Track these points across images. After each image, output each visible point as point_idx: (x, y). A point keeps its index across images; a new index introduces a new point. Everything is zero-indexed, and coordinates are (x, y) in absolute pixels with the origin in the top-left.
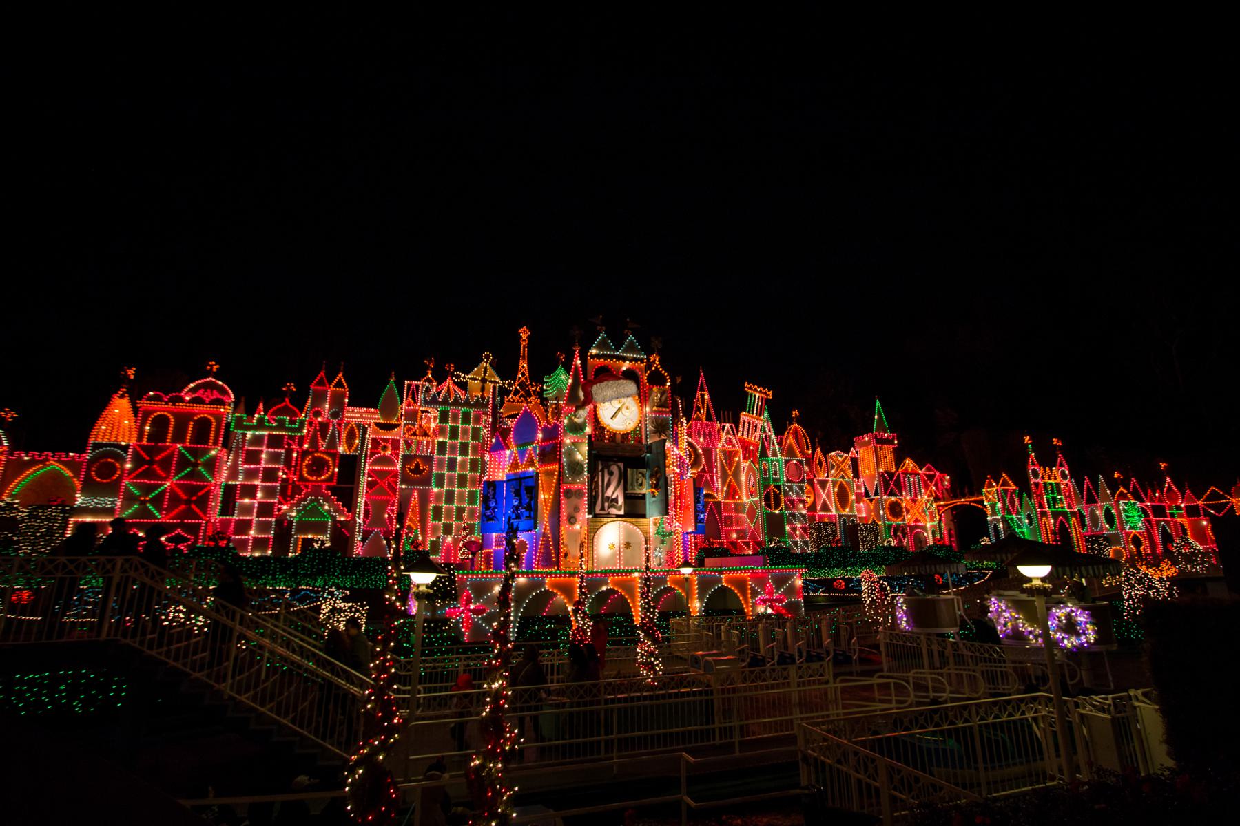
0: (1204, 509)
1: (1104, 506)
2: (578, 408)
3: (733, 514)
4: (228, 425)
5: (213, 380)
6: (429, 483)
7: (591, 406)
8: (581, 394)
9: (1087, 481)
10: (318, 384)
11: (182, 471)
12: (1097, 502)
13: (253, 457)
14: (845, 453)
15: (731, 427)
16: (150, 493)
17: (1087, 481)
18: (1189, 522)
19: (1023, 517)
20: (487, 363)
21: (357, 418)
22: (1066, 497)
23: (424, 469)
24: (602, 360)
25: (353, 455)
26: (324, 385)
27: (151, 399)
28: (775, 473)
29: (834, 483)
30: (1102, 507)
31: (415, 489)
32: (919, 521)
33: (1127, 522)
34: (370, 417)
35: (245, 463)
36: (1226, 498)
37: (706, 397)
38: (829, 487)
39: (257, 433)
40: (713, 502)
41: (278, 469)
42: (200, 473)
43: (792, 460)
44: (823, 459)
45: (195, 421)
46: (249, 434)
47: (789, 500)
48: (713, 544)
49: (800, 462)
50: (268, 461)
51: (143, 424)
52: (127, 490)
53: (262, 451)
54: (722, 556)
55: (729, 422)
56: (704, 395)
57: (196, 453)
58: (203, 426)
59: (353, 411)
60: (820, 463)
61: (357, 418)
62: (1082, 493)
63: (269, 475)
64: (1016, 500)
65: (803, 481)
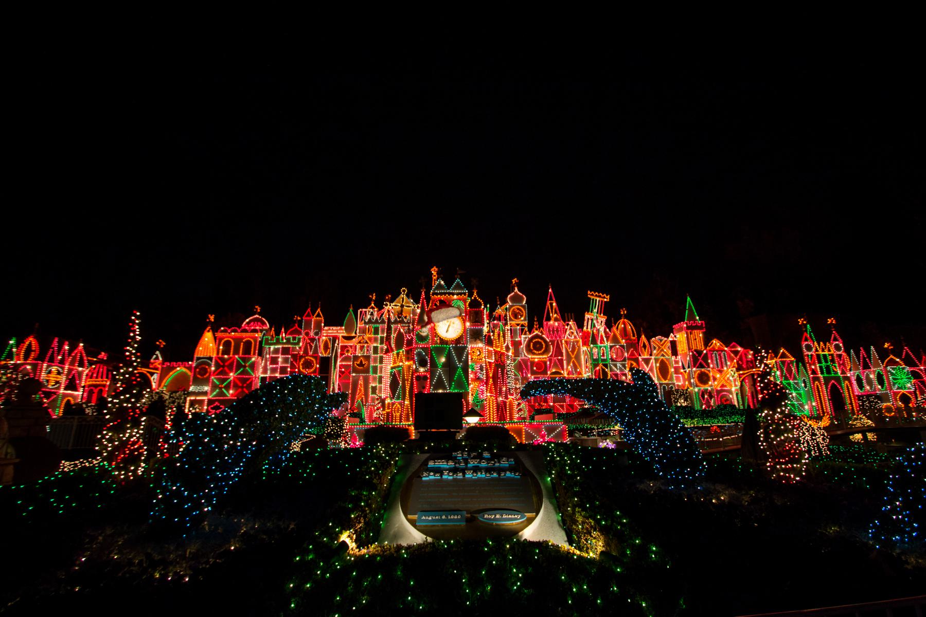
1: (876, 370)
2: (422, 327)
4: (261, 342)
5: (258, 316)
6: (368, 372)
7: (432, 325)
8: (426, 318)
9: (862, 352)
10: (307, 316)
12: (870, 368)
13: (274, 361)
14: (665, 337)
16: (223, 383)
17: (862, 352)
19: (799, 381)
20: (404, 294)
21: (335, 333)
22: (839, 365)
23: (365, 364)
24: (439, 296)
25: (327, 357)
26: (310, 316)
27: (222, 331)
28: (603, 355)
29: (656, 360)
30: (874, 372)
31: (360, 376)
32: (726, 386)
33: (894, 384)
34: (340, 332)
35: (270, 364)
37: (554, 304)
38: (652, 363)
39: (276, 347)
41: (288, 367)
42: (247, 370)
43: (616, 346)
44: (647, 344)
45: (244, 342)
46: (272, 347)
47: (614, 374)
48: (542, 406)
49: (623, 346)
50: (283, 363)
51: (219, 346)
52: (213, 382)
53: (279, 357)
54: (547, 414)
56: (552, 303)
57: (244, 360)
58: (248, 345)
59: (332, 329)
60: (645, 346)
61: (335, 333)
62: (859, 361)
64: (793, 369)
65: (624, 360)
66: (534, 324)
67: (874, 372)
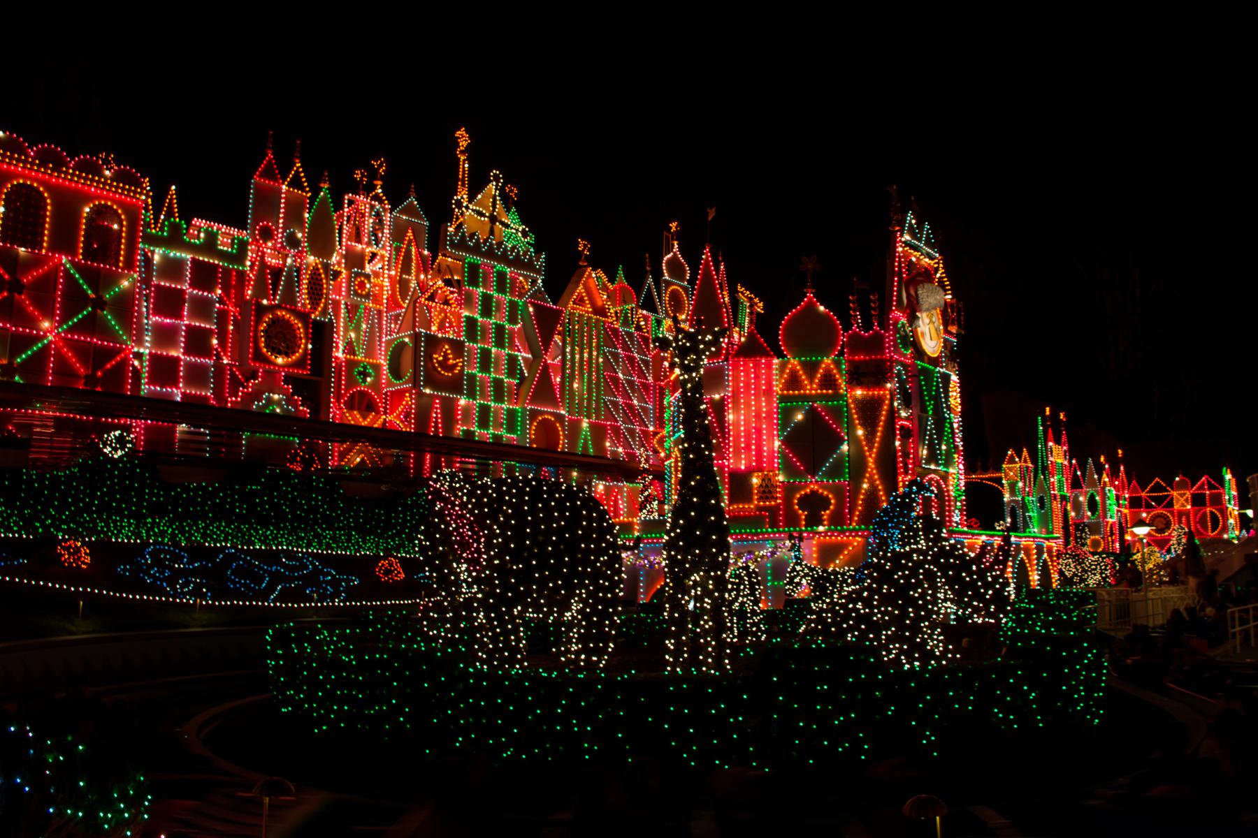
0: (1146, 501)
11: (76, 314)
12: (1082, 488)
18: (1130, 512)
36: (1168, 491)
42: (105, 322)
46: (158, 255)
63: (197, 342)
67: (1086, 493)
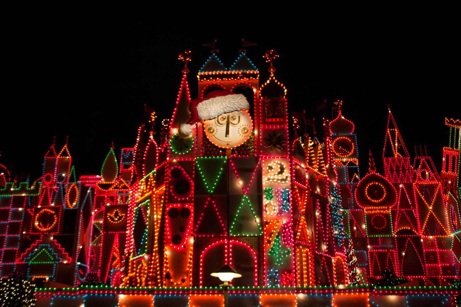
3: (437, 250)
15: (427, 160)
40: (412, 238)
55: (424, 155)
66: (369, 161)
